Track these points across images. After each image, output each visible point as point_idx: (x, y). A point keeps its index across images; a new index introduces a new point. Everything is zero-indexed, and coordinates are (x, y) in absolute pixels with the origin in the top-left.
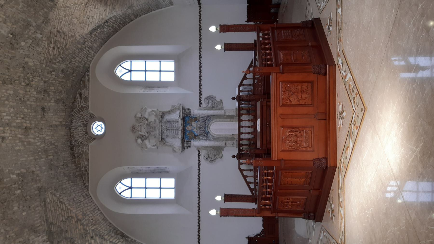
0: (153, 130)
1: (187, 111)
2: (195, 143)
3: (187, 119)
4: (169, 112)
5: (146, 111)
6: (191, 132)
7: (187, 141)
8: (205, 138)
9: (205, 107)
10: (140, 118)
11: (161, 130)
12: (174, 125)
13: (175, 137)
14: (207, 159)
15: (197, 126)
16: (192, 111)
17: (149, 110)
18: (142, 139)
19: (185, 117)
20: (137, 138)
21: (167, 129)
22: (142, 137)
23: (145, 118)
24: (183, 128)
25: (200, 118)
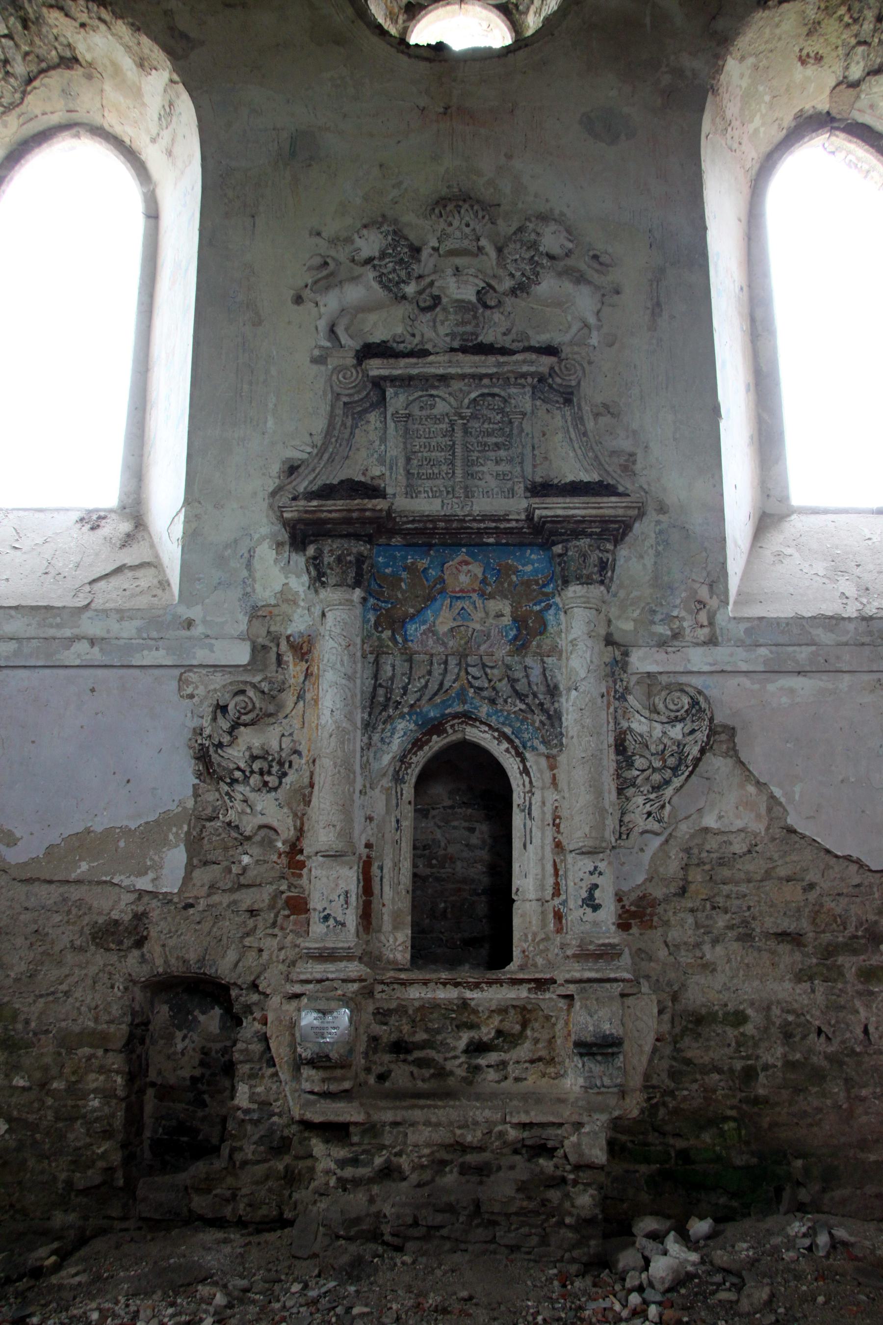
1: (594, 557)
3: (531, 564)
6: (433, 593)
10: (534, 245)
14: (224, 709)
18: (383, 255)
23: (537, 274)
25: (541, 656)
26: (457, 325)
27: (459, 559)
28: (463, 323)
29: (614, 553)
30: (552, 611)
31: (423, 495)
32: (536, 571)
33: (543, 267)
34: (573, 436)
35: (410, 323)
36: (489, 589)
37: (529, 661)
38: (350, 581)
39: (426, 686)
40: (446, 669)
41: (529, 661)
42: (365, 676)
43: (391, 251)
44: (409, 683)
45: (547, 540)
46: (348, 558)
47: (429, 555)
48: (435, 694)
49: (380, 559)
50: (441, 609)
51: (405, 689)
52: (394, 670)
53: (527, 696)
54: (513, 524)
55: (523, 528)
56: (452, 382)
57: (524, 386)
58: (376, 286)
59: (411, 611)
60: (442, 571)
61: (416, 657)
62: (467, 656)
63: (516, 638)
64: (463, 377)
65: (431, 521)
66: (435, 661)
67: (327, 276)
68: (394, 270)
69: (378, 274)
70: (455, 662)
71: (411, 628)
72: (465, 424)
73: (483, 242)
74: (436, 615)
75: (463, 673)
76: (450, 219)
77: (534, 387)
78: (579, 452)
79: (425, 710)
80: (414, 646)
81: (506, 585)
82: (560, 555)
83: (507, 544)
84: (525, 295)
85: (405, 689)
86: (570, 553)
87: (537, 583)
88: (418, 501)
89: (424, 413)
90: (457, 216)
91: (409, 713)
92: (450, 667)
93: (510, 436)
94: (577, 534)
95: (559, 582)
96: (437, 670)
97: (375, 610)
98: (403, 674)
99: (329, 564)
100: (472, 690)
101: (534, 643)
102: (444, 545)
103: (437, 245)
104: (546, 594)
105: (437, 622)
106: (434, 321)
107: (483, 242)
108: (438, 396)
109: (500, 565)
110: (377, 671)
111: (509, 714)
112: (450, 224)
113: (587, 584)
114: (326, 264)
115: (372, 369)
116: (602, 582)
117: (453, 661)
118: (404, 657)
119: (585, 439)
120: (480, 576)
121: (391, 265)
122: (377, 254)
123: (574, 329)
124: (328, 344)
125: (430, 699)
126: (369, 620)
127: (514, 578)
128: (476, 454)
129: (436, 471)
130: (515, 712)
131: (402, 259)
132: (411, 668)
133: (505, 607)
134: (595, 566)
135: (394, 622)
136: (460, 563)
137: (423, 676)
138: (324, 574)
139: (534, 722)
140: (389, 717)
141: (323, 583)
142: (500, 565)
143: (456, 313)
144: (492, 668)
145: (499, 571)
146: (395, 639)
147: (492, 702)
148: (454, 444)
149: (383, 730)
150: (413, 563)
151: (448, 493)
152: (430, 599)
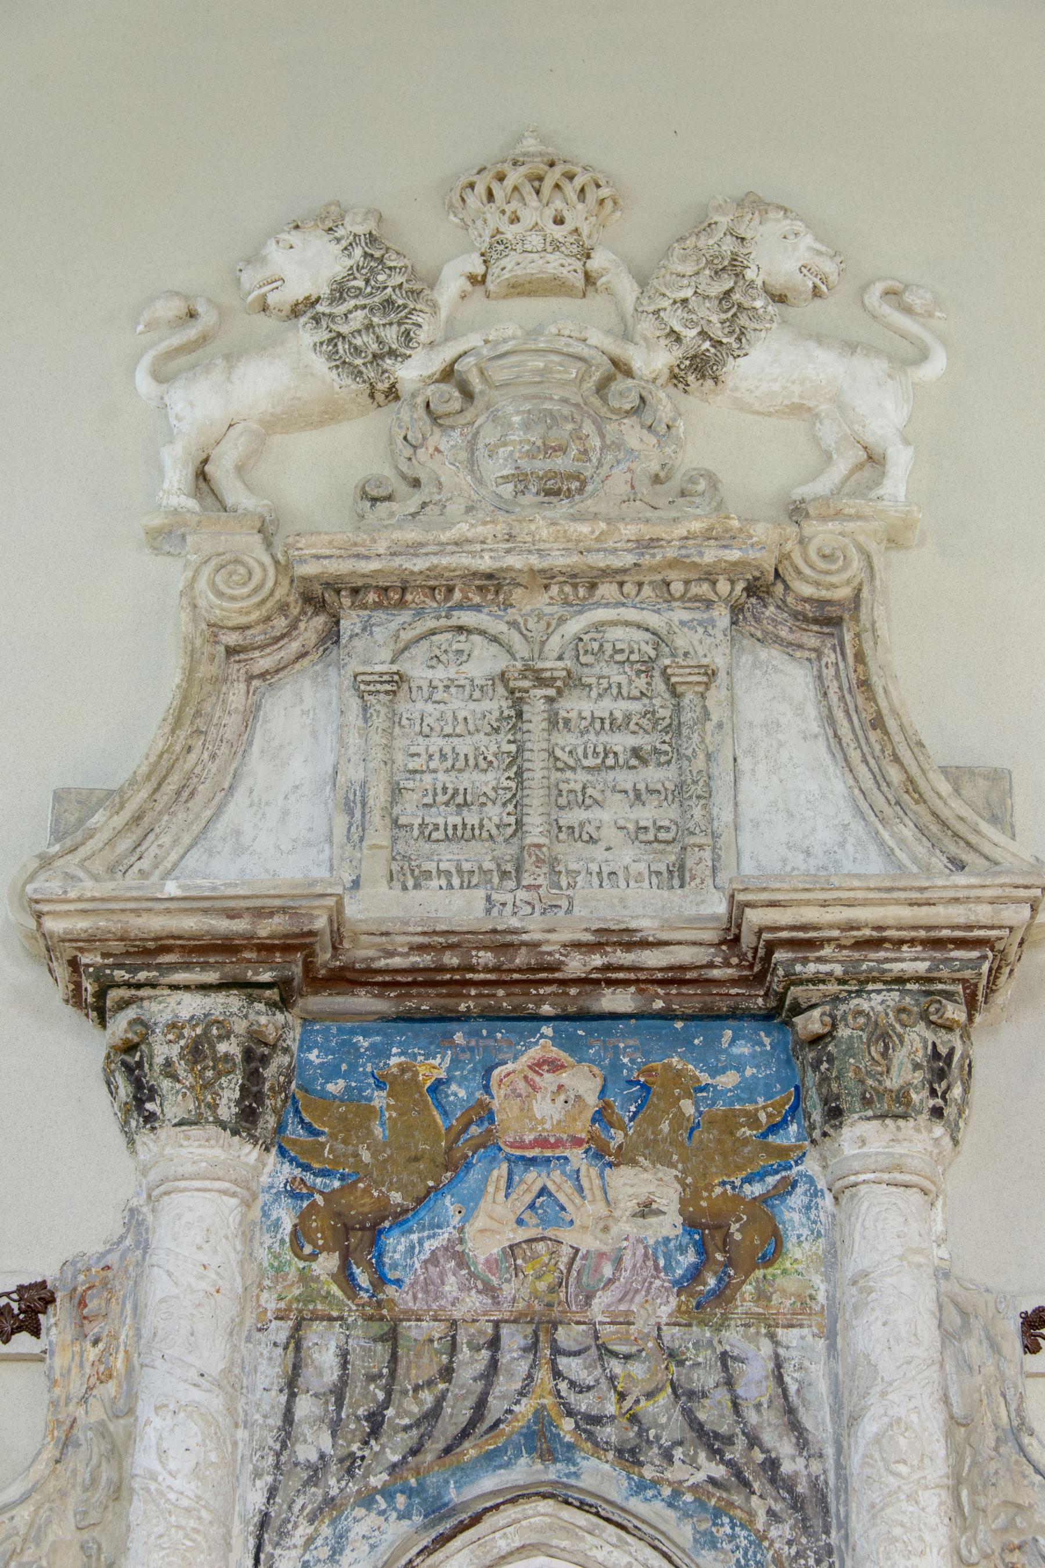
0: (496, 468)
1: (917, 1039)
2: (203, 1222)
3: (739, 1065)
4: (863, 720)
5: (851, 347)
6: (458, 1150)
7: (255, 1055)
8: (313, 1443)
9: (1017, 1431)
10: (735, 267)
11: (492, 584)
12: (611, 814)
13: (356, 835)
15: (577, 1278)
16: (916, 1140)
17: (882, 409)
18: (340, 291)
19: (779, 1013)
20: (357, 225)
21: (523, 688)
22: (369, 311)
24: (543, 973)
25: (769, 1325)
26: (531, 456)
27: (534, 1053)
28: (550, 450)
29: (966, 1036)
30: (797, 1199)
31: (435, 883)
32: (749, 1089)
33: (759, 318)
34: (845, 731)
35: (408, 452)
36: (618, 1137)
37: (733, 1338)
38: (227, 1111)
39: (434, 1413)
40: (494, 1365)
41: (733, 1338)
42: (262, 1381)
43: (361, 283)
44: (387, 1403)
45: (782, 997)
46: (222, 1048)
47: (453, 1046)
48: (465, 1434)
49: (313, 1056)
50: (480, 1192)
51: (376, 1423)
52: (344, 1365)
53: (729, 1440)
54: (684, 955)
55: (711, 965)
56: (518, 593)
57: (709, 604)
58: (320, 364)
59: (396, 1197)
60: (487, 1088)
61: (412, 1331)
62: (555, 1325)
63: (695, 1274)
64: (545, 578)
65: (451, 947)
66: (462, 1338)
67: (195, 342)
68: (369, 327)
69: (326, 336)
70: (522, 1343)
71: (396, 1246)
72: (550, 700)
73: (598, 261)
74: (469, 1207)
75: (543, 1374)
76: (515, 205)
77: (736, 610)
78: (862, 770)
79: (431, 1480)
80: (403, 1298)
81: (665, 1127)
82: (816, 1040)
83: (667, 1015)
84: (709, 383)
85: (376, 1423)
86: (843, 1032)
87: (753, 1120)
88: (420, 895)
89: (440, 674)
90: (532, 200)
91: (388, 1493)
92: (504, 1359)
93: (675, 728)
94: (860, 982)
95: (817, 1116)
96: (470, 1365)
97: (294, 1195)
98: (372, 1378)
99: (168, 1063)
100: (568, 1424)
101: (748, 1288)
102: (493, 1016)
103: (480, 270)
104: (783, 1152)
105: (470, 1230)
106: (472, 446)
107: (598, 261)
108: (482, 633)
109: (648, 1072)
110: (297, 1367)
111: (677, 1494)
112: (515, 219)
113: (896, 1117)
114: (192, 315)
115: (302, 561)
116: (937, 1113)
117: (513, 1339)
118: (377, 1328)
119: (874, 736)
120: (592, 1100)
121: (360, 314)
122: (325, 291)
123: (841, 467)
124: (192, 503)
125: (448, 1450)
126: (277, 1225)
127: (688, 1107)
128: (582, 777)
129: (472, 819)
130: (694, 1488)
131: (389, 302)
132: (394, 1358)
133: (658, 1185)
134: (917, 1066)
135: (348, 1229)
136: (537, 1066)
137: (430, 1383)
138: (153, 1093)
139: (751, 1514)
140: (329, 1502)
141: (150, 1118)
142: (648, 1072)
143: (527, 426)
144: (627, 1357)
145: (646, 1087)
146: (351, 1277)
147: (629, 1456)
148: (520, 750)
149: (310, 1541)
150: (403, 1069)
151: (504, 875)
152: (454, 1164)
